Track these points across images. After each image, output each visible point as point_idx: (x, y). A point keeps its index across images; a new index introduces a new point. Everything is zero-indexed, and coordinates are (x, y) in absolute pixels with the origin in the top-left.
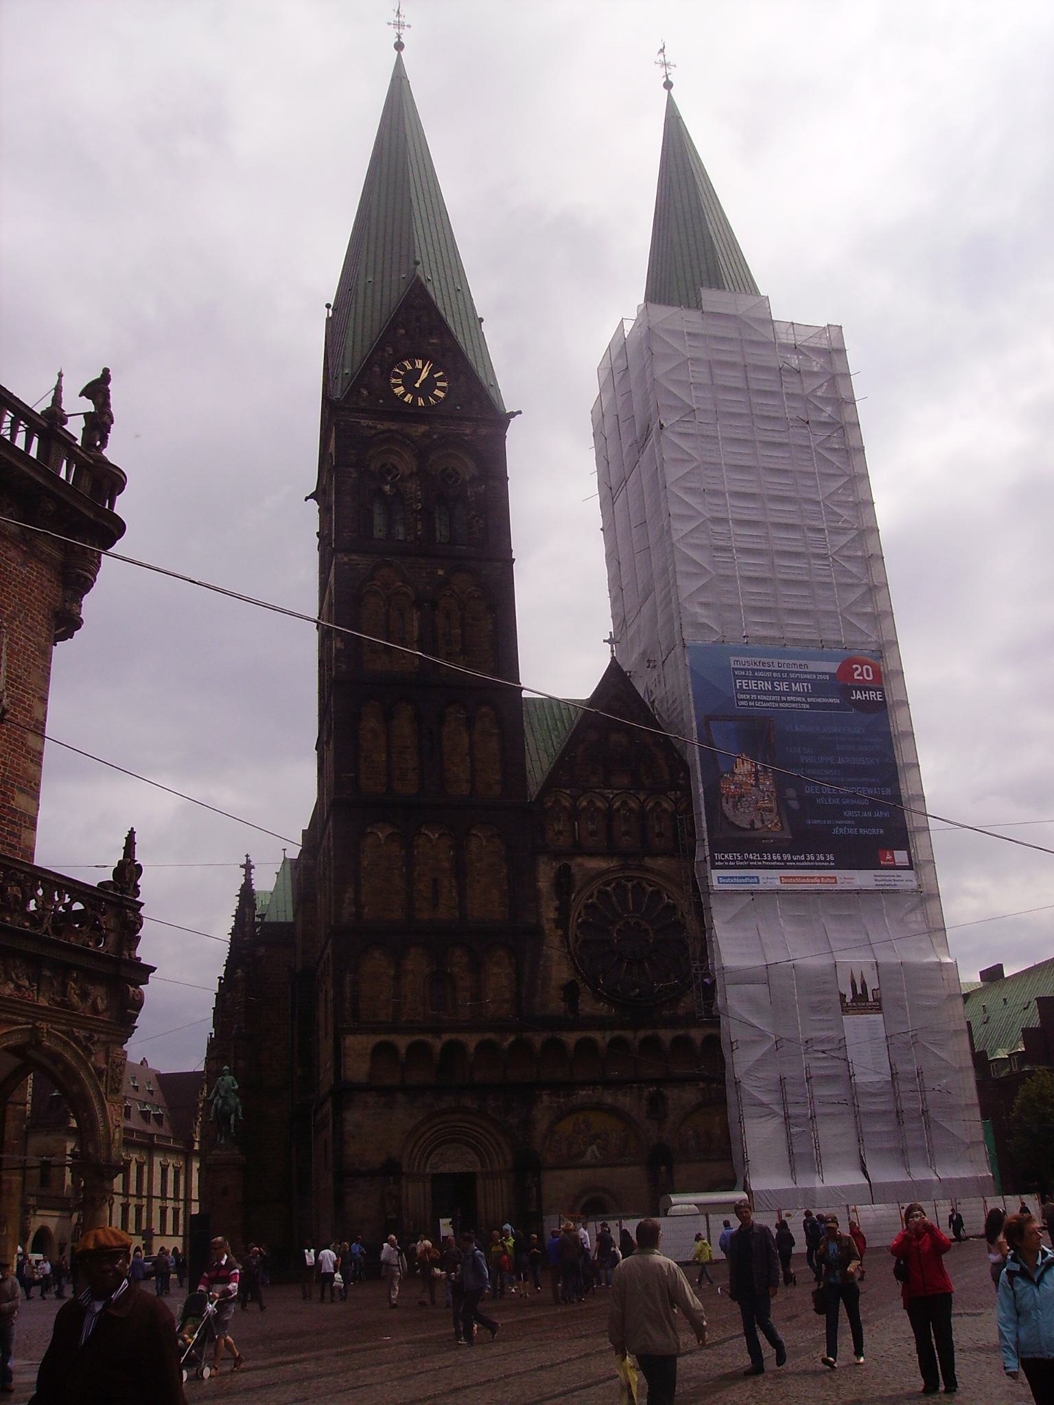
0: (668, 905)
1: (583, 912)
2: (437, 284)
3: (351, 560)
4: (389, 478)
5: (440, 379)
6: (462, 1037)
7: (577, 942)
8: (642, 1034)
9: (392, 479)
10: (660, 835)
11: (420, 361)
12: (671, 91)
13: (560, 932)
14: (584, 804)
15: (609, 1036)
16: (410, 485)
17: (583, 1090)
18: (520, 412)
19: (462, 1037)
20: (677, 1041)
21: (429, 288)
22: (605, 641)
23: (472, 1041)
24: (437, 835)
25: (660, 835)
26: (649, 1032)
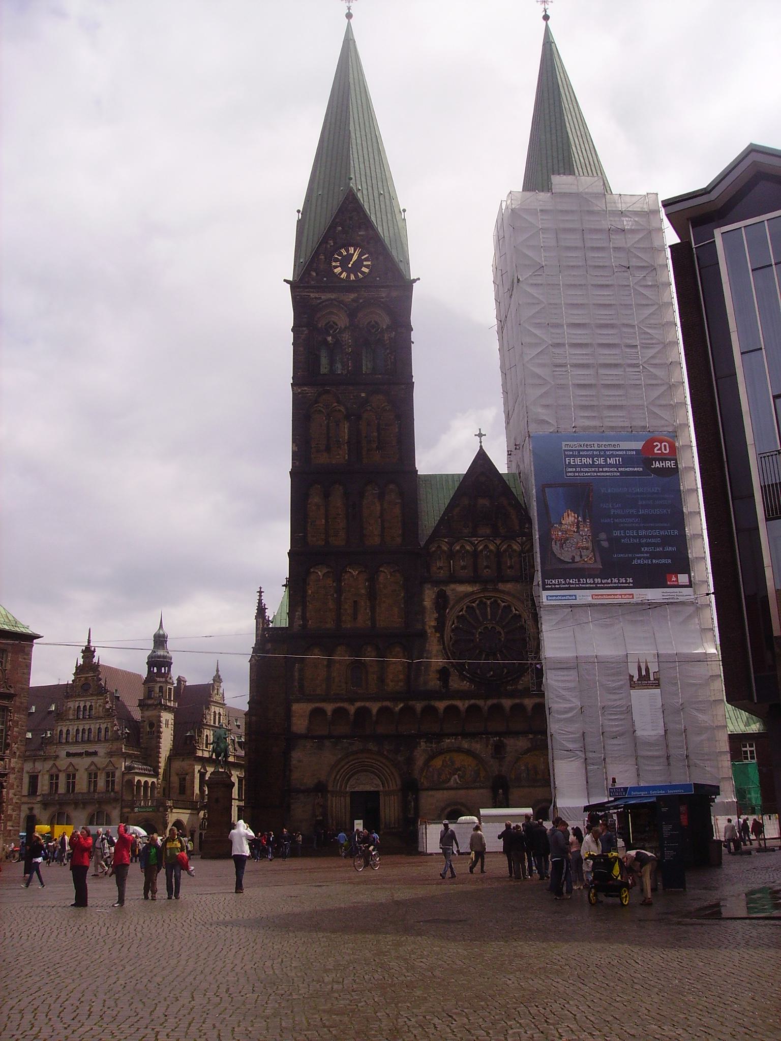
0: (515, 614)
1: (455, 620)
2: (365, 192)
3: (303, 390)
4: (331, 332)
5: (366, 260)
6: (367, 704)
7: (451, 641)
8: (490, 702)
9: (333, 332)
10: (511, 567)
11: (353, 248)
12: (548, 22)
13: (438, 635)
14: (458, 548)
15: (467, 703)
16: (344, 335)
17: (448, 739)
18: (419, 279)
19: (367, 704)
20: (514, 707)
21: (359, 195)
22: (475, 435)
23: (375, 707)
24: (357, 572)
25: (511, 567)
26: (495, 701)
